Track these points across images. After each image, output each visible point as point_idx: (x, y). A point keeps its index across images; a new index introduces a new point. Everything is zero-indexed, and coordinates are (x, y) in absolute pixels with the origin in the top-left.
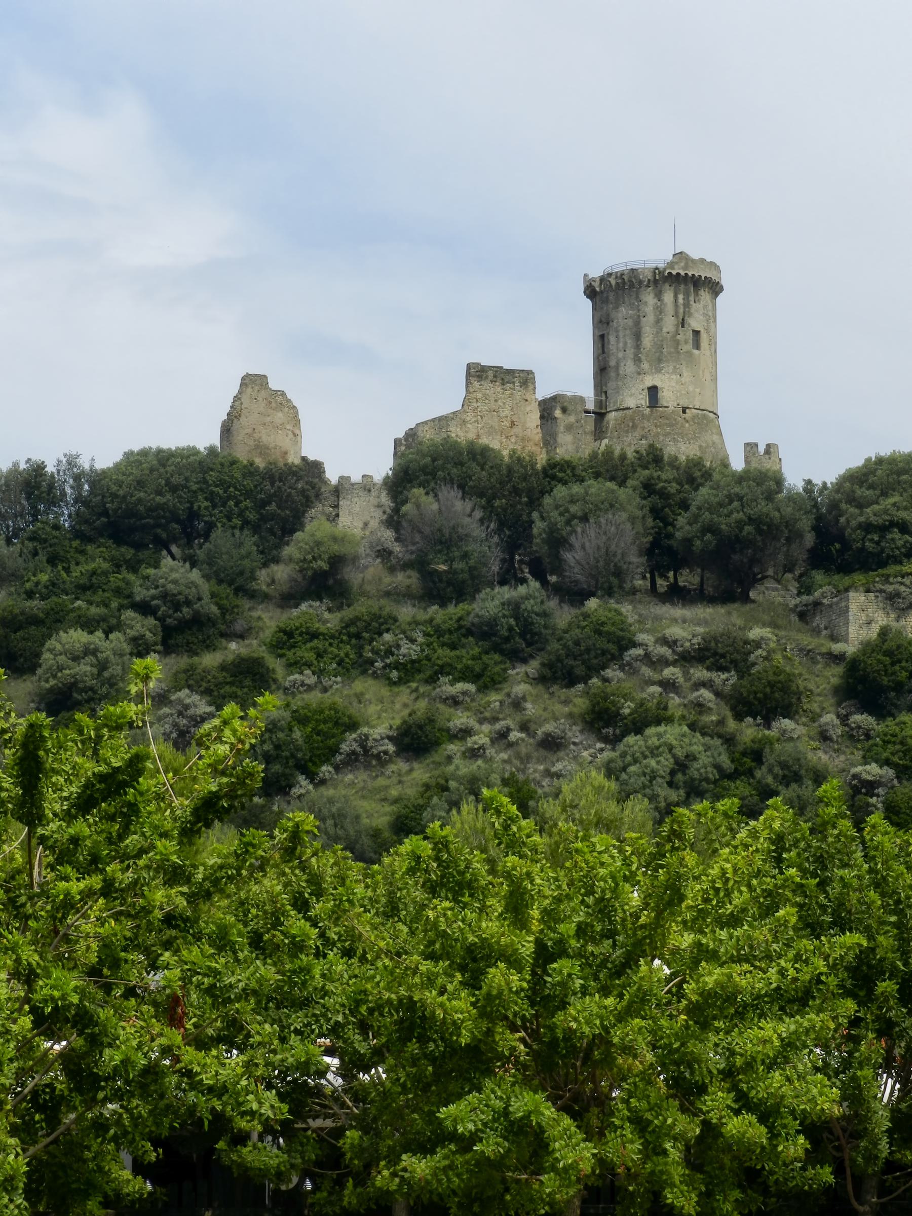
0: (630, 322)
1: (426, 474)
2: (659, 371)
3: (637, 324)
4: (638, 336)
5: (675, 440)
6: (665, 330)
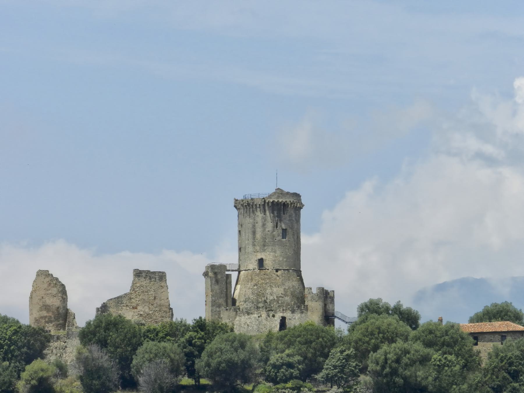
0: (250, 226)
1: (91, 334)
2: (264, 251)
3: (254, 226)
4: (254, 233)
5: (271, 286)
6: (267, 230)
